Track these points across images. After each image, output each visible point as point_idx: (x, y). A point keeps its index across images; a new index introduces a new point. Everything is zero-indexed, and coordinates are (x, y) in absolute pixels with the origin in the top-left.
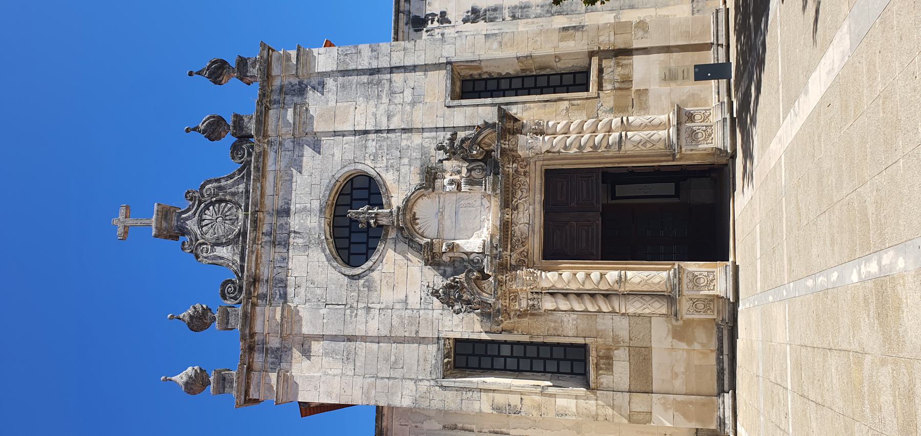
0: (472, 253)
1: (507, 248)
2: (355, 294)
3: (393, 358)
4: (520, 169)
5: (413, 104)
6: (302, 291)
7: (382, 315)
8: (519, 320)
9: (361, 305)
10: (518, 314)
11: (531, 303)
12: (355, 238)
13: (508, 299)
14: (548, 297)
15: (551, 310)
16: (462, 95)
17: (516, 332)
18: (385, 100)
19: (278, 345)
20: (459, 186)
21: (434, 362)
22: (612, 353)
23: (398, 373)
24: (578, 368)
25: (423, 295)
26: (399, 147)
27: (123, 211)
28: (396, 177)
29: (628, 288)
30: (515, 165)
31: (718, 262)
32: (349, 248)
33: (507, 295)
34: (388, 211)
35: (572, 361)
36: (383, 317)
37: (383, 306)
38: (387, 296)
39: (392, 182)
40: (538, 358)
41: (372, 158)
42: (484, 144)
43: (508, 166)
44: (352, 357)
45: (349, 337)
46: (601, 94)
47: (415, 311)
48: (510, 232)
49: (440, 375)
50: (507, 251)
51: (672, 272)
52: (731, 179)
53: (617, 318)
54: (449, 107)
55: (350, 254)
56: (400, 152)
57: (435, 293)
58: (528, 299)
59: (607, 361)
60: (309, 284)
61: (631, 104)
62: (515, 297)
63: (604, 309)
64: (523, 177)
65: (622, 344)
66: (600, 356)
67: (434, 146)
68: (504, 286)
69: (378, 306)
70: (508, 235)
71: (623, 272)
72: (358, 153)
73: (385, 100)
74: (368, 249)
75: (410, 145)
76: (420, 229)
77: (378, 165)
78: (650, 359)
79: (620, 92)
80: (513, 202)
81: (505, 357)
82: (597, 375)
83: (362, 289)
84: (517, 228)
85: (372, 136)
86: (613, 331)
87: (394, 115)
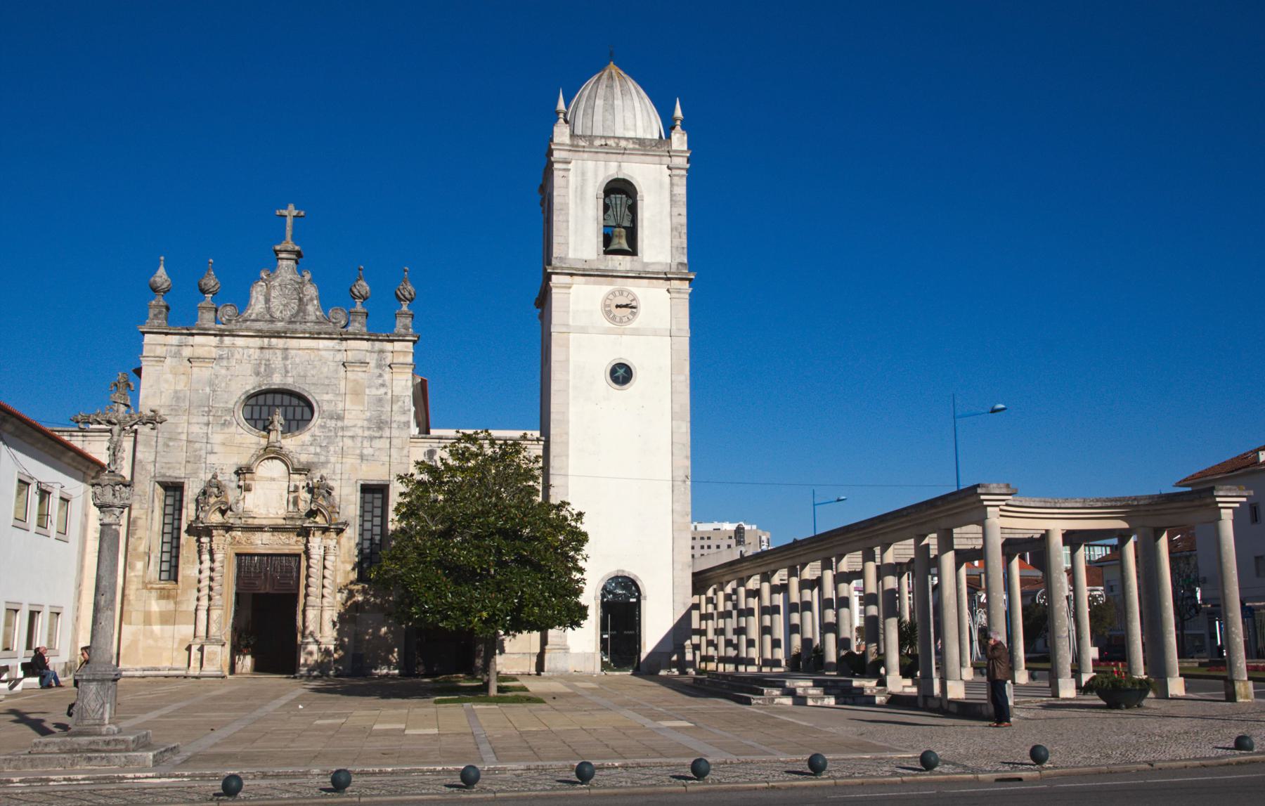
2: (220, 413)
3: (171, 444)
5: (362, 457)
6: (223, 372)
9: (211, 418)
12: (265, 409)
18: (367, 433)
19: (184, 355)
20: (294, 492)
21: (168, 474)
23: (159, 448)
24: (165, 575)
25: (216, 466)
28: (307, 443)
32: (257, 405)
37: (210, 435)
38: (217, 438)
44: (173, 413)
49: (158, 479)
54: (356, 482)
55: (252, 406)
57: (215, 477)
60: (229, 377)
72: (326, 413)
73: (367, 433)
74: (256, 420)
77: (316, 429)
83: (223, 419)
87: (353, 441)
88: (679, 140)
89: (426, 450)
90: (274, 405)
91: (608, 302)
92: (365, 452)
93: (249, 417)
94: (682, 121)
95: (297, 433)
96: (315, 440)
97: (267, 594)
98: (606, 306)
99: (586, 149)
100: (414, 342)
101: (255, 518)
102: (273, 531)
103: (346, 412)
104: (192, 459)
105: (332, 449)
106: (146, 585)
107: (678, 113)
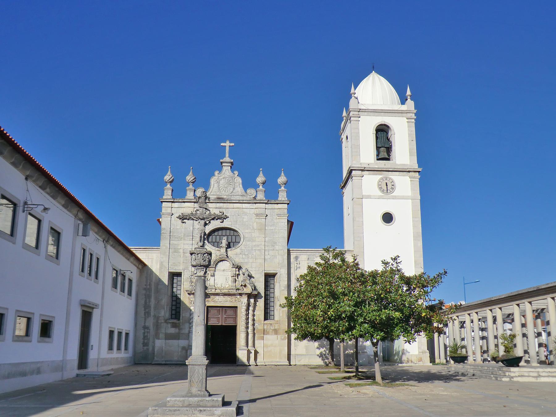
4: (237, 298)
16: (269, 275)
24: (173, 316)
27: (232, 144)
39: (236, 251)
41: (246, 244)
59: (174, 326)
74: (214, 242)
82: (170, 323)
88: (410, 105)
89: (295, 256)
90: (222, 235)
91: (380, 183)
94: (411, 96)
95: (233, 249)
97: (222, 325)
98: (379, 185)
99: (366, 111)
100: (288, 204)
102: (224, 295)
104: (185, 261)
105: (250, 256)
106: (166, 321)
107: (409, 93)
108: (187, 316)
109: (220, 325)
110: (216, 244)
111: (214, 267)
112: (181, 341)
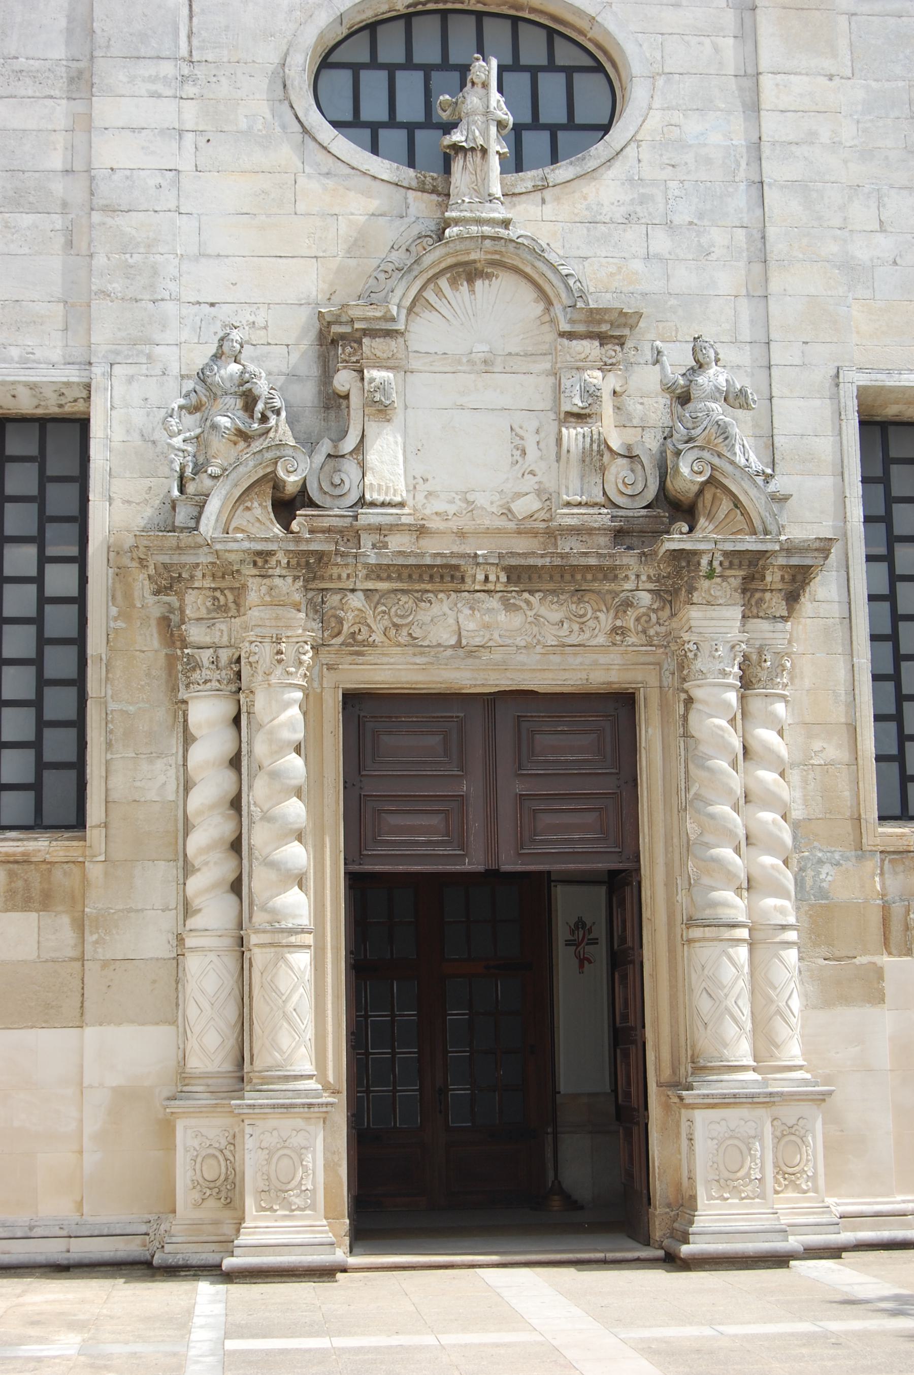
0: (362, 465)
1: (379, 578)
4: (632, 614)
7: (159, 180)
8: (153, 623)
10: (172, 616)
11: (205, 656)
13: (213, 586)
14: (229, 709)
15: (186, 721)
17: (114, 611)
20: (580, 417)
22: (60, 908)
25: (224, 313)
26: (706, 222)
29: (259, 957)
30: (645, 598)
31: (347, 1221)
32: (374, 64)
33: (228, 582)
34: (497, 190)
35: (36, 787)
36: (152, 182)
40: (42, 682)
42: (714, 497)
43: (644, 578)
45: (86, 75)
46: (872, 864)
47: (172, 286)
48: (428, 587)
50: (367, 577)
51: (312, 1084)
52: (600, 1255)
53: (168, 921)
55: (356, 68)
56: (691, 223)
58: (216, 647)
61: (838, 954)
62: (224, 609)
63: (194, 884)
64: (609, 628)
65: (90, 938)
66: (50, 871)
67: (709, 333)
68: (255, 572)
69: (188, 165)
70: (421, 579)
71: (309, 939)
74: (374, 127)
75: (713, 257)
76: (439, 292)
78: (47, 1024)
79: (875, 918)
80: (526, 595)
81: (39, 580)
84: (446, 609)
85: (738, 126)
86: (130, 910)
92: (861, 251)
93: (348, 117)
95: (563, 172)
96: (643, 200)
97: (493, 876)
101: (421, 531)
103: (767, 82)
108: (152, 795)
109: (481, 868)
110: (393, 138)
111: (401, 326)
112: (110, 1031)
